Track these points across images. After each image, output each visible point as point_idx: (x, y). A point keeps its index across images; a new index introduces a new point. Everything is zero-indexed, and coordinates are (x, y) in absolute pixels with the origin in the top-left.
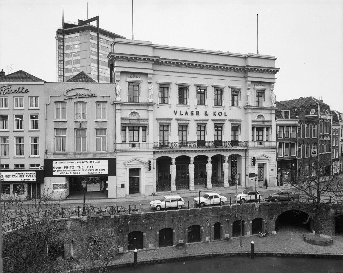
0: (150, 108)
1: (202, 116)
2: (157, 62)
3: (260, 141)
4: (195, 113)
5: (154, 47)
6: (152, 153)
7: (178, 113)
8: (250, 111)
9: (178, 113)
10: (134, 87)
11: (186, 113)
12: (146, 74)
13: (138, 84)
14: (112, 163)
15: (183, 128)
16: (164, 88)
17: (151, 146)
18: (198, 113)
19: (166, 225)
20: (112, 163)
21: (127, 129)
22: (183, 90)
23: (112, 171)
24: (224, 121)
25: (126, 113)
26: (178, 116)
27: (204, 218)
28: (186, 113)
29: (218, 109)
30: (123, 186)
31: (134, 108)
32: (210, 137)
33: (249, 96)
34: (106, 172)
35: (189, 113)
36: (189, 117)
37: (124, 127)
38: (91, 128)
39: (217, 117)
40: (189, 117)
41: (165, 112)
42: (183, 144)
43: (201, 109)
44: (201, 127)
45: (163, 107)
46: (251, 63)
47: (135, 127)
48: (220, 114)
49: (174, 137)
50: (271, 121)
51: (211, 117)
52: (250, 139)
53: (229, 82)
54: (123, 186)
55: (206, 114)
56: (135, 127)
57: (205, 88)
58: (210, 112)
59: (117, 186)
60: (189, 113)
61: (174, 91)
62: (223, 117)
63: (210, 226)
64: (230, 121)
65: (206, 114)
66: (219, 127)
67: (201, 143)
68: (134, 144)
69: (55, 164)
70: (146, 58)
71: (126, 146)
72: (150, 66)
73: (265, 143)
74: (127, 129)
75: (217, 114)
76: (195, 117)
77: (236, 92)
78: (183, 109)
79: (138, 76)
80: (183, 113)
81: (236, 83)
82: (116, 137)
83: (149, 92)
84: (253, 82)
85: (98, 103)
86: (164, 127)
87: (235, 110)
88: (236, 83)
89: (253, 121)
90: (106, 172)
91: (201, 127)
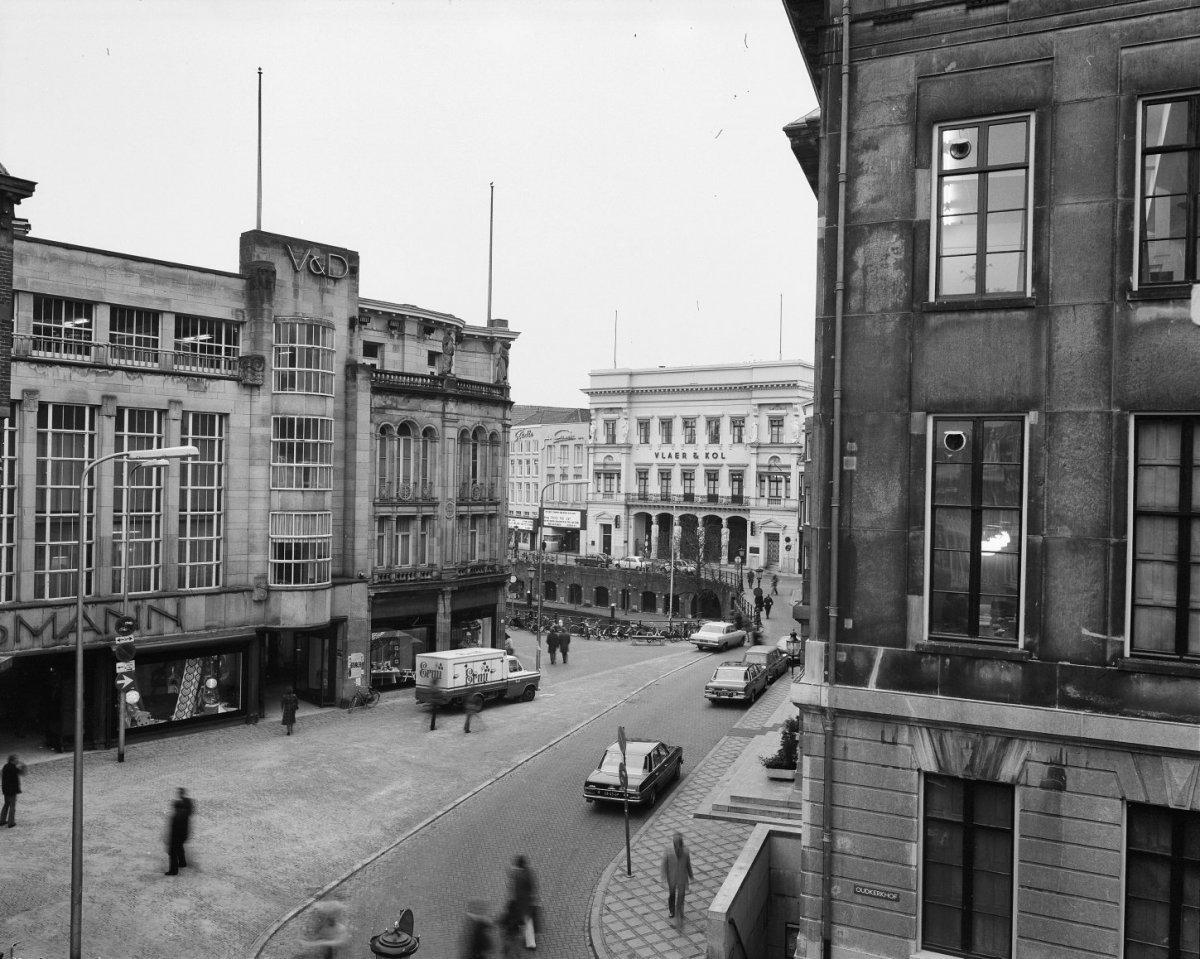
0: (624, 451)
1: (690, 460)
3: (775, 499)
4: (681, 456)
5: (631, 375)
6: (623, 507)
7: (660, 456)
8: (754, 451)
9: (660, 456)
10: (611, 425)
11: (670, 456)
13: (614, 422)
14: (584, 514)
15: (665, 475)
16: (644, 424)
17: (622, 498)
18: (684, 455)
19: (576, 580)
20: (584, 514)
21: (602, 476)
22: (666, 423)
23: (584, 526)
24: (721, 465)
25: (600, 458)
26: (660, 460)
27: (612, 580)
28: (670, 456)
29: (714, 448)
30: (593, 543)
31: (608, 450)
32: (700, 488)
33: (757, 429)
34: (578, 526)
35: (673, 455)
36: (673, 460)
37: (597, 474)
38: (571, 472)
39: (711, 461)
40: (673, 460)
41: (644, 455)
42: (666, 497)
43: (690, 450)
44: (688, 475)
45: (645, 448)
46: (759, 377)
47: (608, 474)
48: (715, 455)
49: (654, 487)
51: (702, 460)
53: (726, 409)
54: (593, 543)
55: (696, 456)
56: (608, 474)
57: (694, 419)
58: (702, 455)
59: (590, 543)
60: (673, 455)
61: (655, 426)
62: (719, 461)
63: (617, 592)
65: (696, 456)
66: (712, 476)
67: (713, 498)
68: (608, 494)
69: (546, 514)
71: (600, 497)
72: (625, 398)
74: (602, 476)
75: (710, 456)
76: (681, 461)
77: (738, 423)
78: (667, 450)
80: (666, 455)
82: (591, 487)
83: (626, 429)
84: (760, 405)
85: (578, 446)
86: (642, 475)
88: (738, 410)
90: (578, 526)
91: (688, 475)
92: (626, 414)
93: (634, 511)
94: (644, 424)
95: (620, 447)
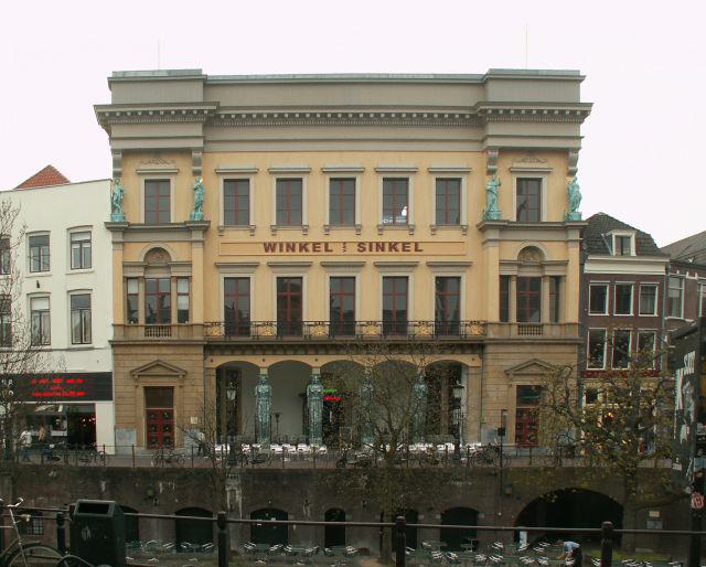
0: (197, 236)
2: (213, 119)
6: (201, 350)
8: (493, 235)
12: (186, 152)
50: (565, 264)
52: (494, 316)
53: (424, 161)
64: (430, 265)
70: (340, 111)
73: (545, 327)
79: (165, 158)
81: (450, 159)
87: (451, 234)
88: (450, 159)
89: (502, 264)
92: (197, 162)
93: (220, 360)
94: (237, 187)
95: (187, 228)
